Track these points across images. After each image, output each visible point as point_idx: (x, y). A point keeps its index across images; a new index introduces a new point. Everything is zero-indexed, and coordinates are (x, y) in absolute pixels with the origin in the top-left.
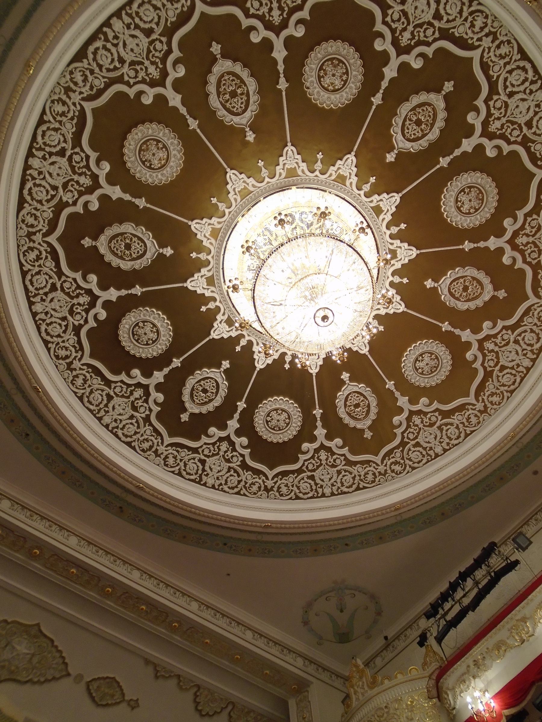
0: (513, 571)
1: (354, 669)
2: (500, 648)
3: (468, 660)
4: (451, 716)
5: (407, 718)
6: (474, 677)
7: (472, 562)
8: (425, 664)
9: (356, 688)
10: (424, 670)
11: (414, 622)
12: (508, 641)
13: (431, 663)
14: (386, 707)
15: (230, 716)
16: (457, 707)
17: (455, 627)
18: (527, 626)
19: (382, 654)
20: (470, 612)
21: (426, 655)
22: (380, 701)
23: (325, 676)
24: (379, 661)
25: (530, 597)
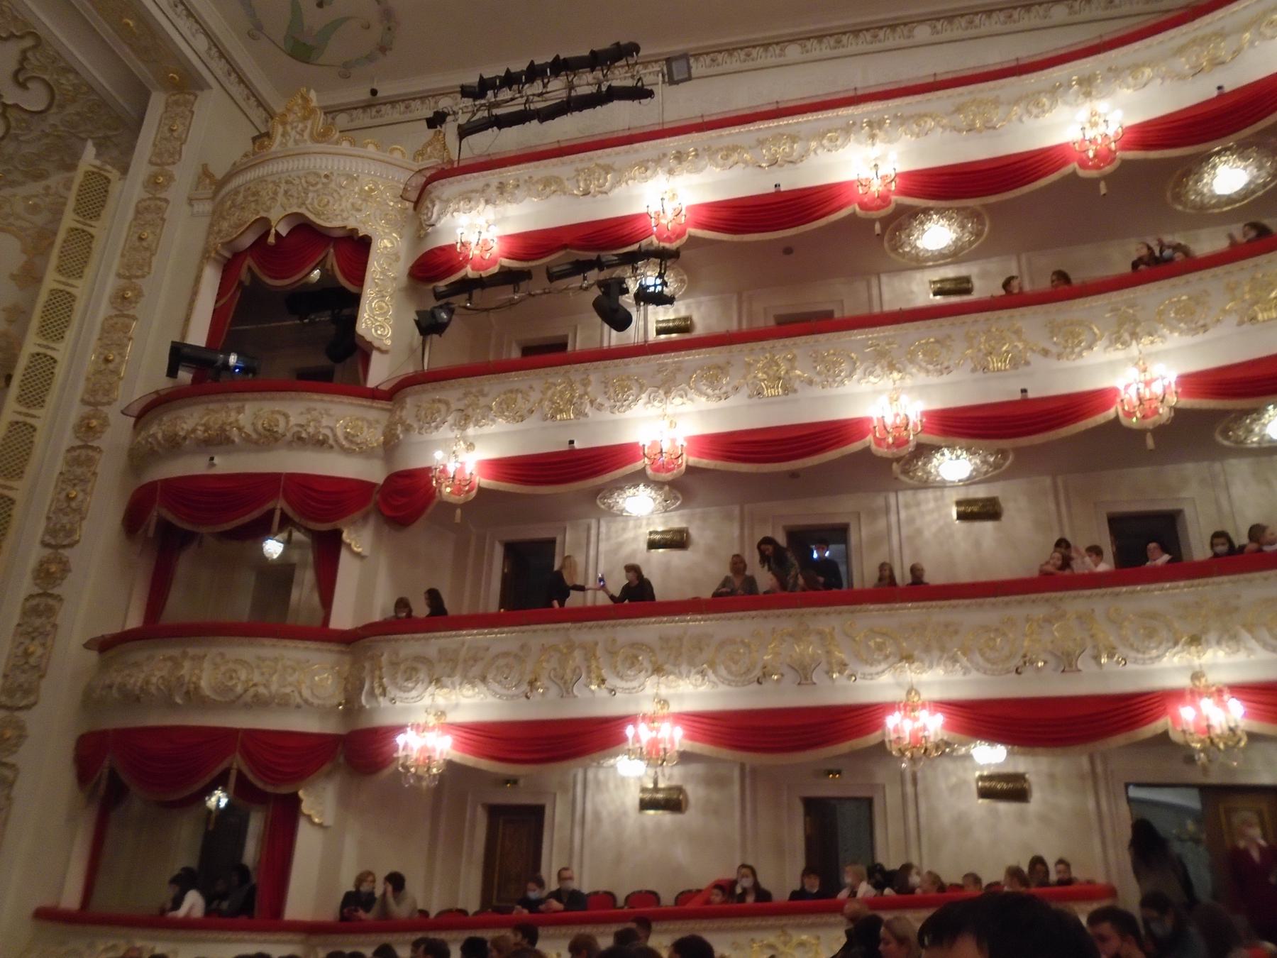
0: (636, 102)
1: (300, 101)
2: (550, 185)
3: (493, 177)
4: (422, 232)
5: (353, 205)
6: (487, 202)
7: (586, 53)
8: (420, 154)
9: (289, 128)
10: (414, 159)
11: (433, 96)
12: (566, 183)
13: (430, 157)
14: (326, 176)
15: (24, 58)
16: (438, 225)
17: (500, 128)
18: (606, 179)
19: (355, 112)
20: (535, 122)
21: (429, 144)
22: (323, 164)
23: (237, 91)
24: (342, 119)
25: (637, 145)
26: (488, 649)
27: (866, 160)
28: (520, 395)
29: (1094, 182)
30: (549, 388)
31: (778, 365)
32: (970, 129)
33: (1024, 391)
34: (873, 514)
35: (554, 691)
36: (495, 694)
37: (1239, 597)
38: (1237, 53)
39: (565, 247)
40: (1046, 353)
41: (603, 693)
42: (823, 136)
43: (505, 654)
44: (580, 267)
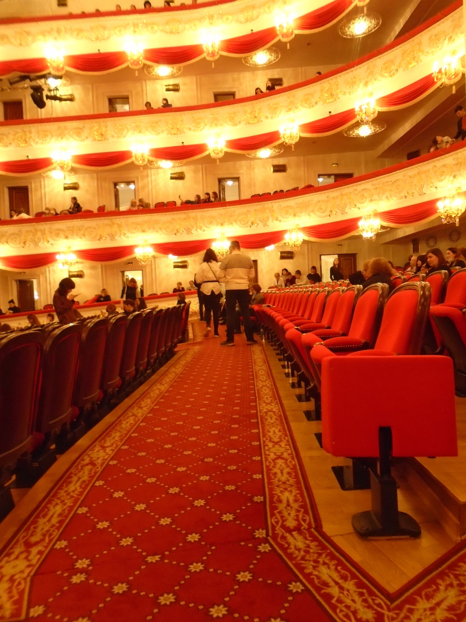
26: (7, 232)
27: (132, 40)
28: (5, 137)
29: (210, 62)
30: (16, 134)
31: (101, 129)
32: (171, 32)
33: (183, 143)
34: (143, 178)
35: (32, 245)
36: (12, 247)
37: (234, 212)
38: (257, 17)
39: (15, 70)
40: (190, 129)
41: (48, 245)
42: (115, 28)
43: (13, 234)
44: (23, 78)
